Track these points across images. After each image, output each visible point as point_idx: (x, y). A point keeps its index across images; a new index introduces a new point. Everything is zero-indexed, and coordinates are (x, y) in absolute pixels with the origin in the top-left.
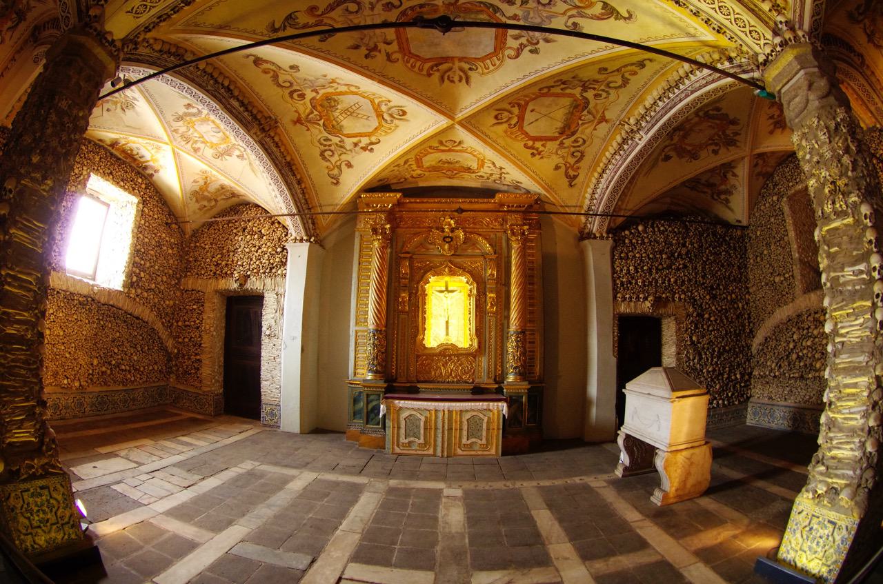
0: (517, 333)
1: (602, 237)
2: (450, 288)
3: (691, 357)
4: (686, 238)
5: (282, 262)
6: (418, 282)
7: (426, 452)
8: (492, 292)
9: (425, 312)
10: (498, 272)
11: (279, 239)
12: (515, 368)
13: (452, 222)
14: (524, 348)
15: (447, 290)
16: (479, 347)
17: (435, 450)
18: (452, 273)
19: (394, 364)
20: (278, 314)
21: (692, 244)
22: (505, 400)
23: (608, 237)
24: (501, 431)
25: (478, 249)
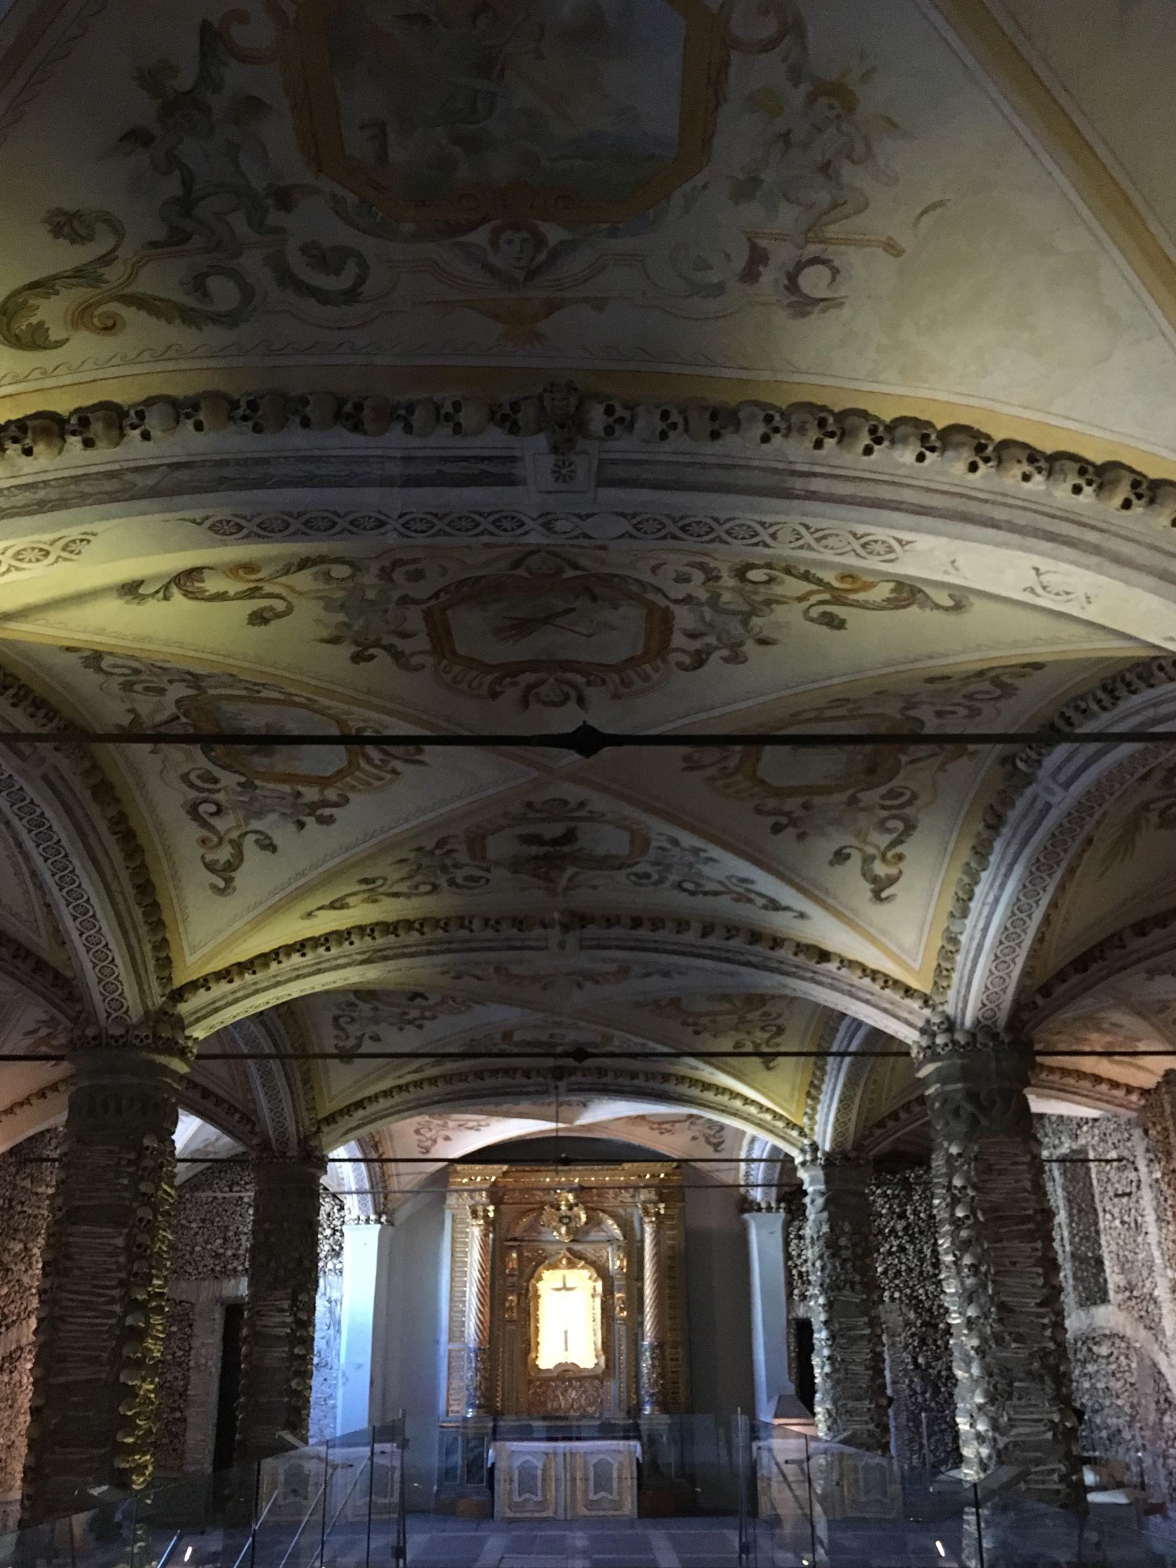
0: (651, 1344)
1: (769, 1209)
2: (568, 1285)
3: (918, 1389)
4: (906, 1204)
5: (333, 1250)
6: (528, 1281)
7: (544, 1514)
8: (619, 1291)
9: (537, 1321)
10: (628, 1262)
11: (329, 1215)
12: (652, 1395)
13: (571, 1197)
14: (663, 1367)
15: (565, 1288)
16: (607, 1366)
17: (556, 1511)
18: (571, 1265)
19: (499, 1394)
20: (332, 1332)
21: (916, 1213)
22: (639, 1438)
23: (778, 1208)
24: (635, 1482)
25: (603, 1231)
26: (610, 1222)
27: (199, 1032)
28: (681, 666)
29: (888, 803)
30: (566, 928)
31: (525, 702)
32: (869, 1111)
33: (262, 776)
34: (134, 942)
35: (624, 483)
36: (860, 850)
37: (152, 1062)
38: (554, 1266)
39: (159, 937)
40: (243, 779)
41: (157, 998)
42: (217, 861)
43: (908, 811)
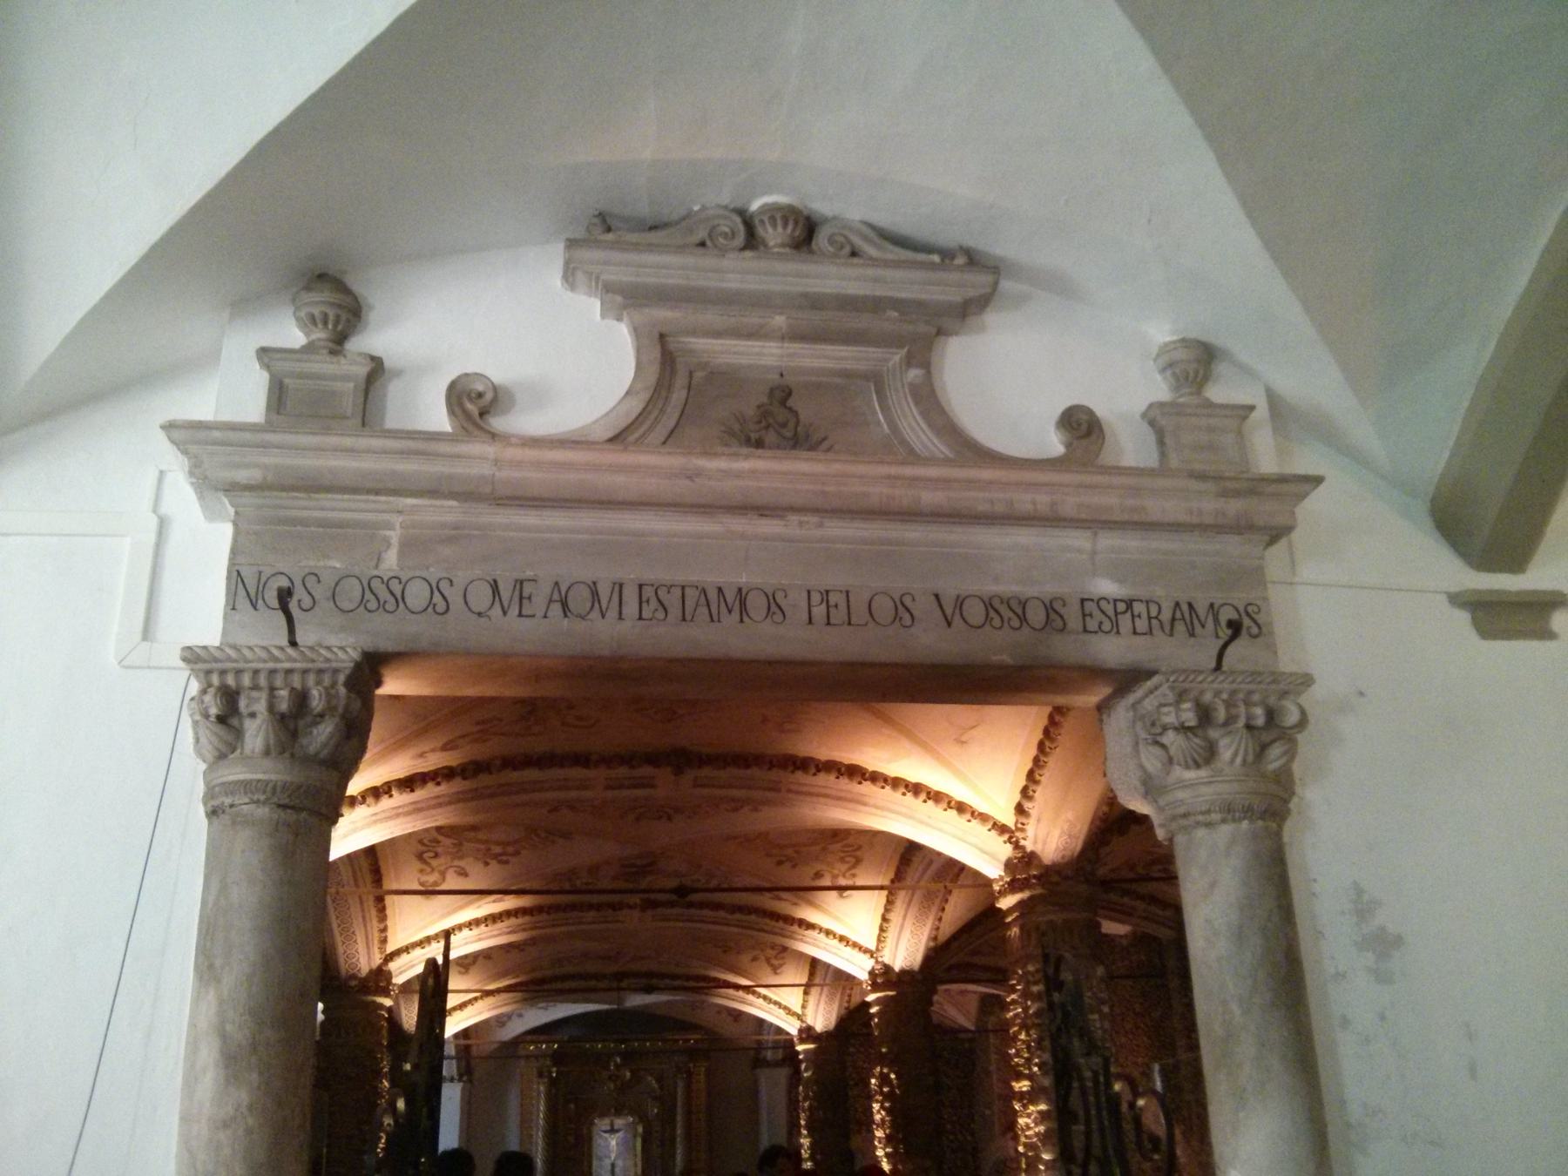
13: (618, 1060)
15: (613, 1131)
26: (650, 1078)
27: (399, 980)
28: (727, 810)
29: (846, 849)
30: (643, 909)
31: (638, 819)
32: (849, 1002)
33: (469, 841)
34: (369, 928)
35: (703, 786)
36: (831, 872)
37: (374, 1002)
38: (602, 1115)
39: (382, 926)
40: (456, 841)
41: (377, 960)
42: (427, 882)
43: (859, 853)
